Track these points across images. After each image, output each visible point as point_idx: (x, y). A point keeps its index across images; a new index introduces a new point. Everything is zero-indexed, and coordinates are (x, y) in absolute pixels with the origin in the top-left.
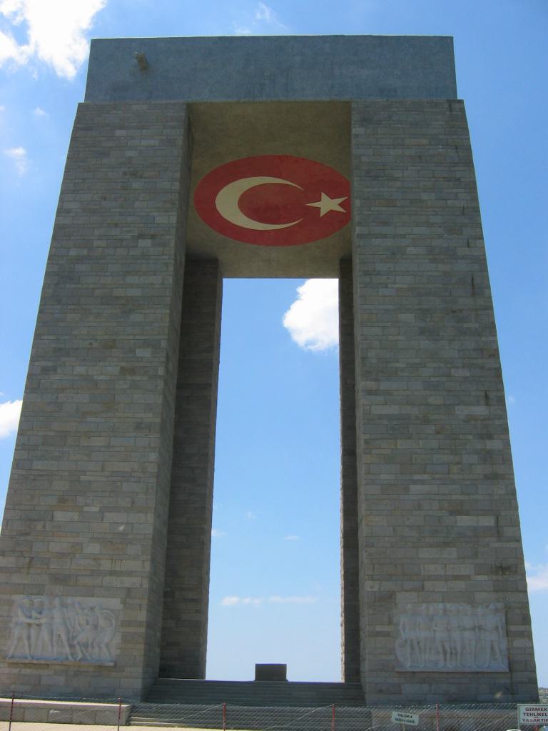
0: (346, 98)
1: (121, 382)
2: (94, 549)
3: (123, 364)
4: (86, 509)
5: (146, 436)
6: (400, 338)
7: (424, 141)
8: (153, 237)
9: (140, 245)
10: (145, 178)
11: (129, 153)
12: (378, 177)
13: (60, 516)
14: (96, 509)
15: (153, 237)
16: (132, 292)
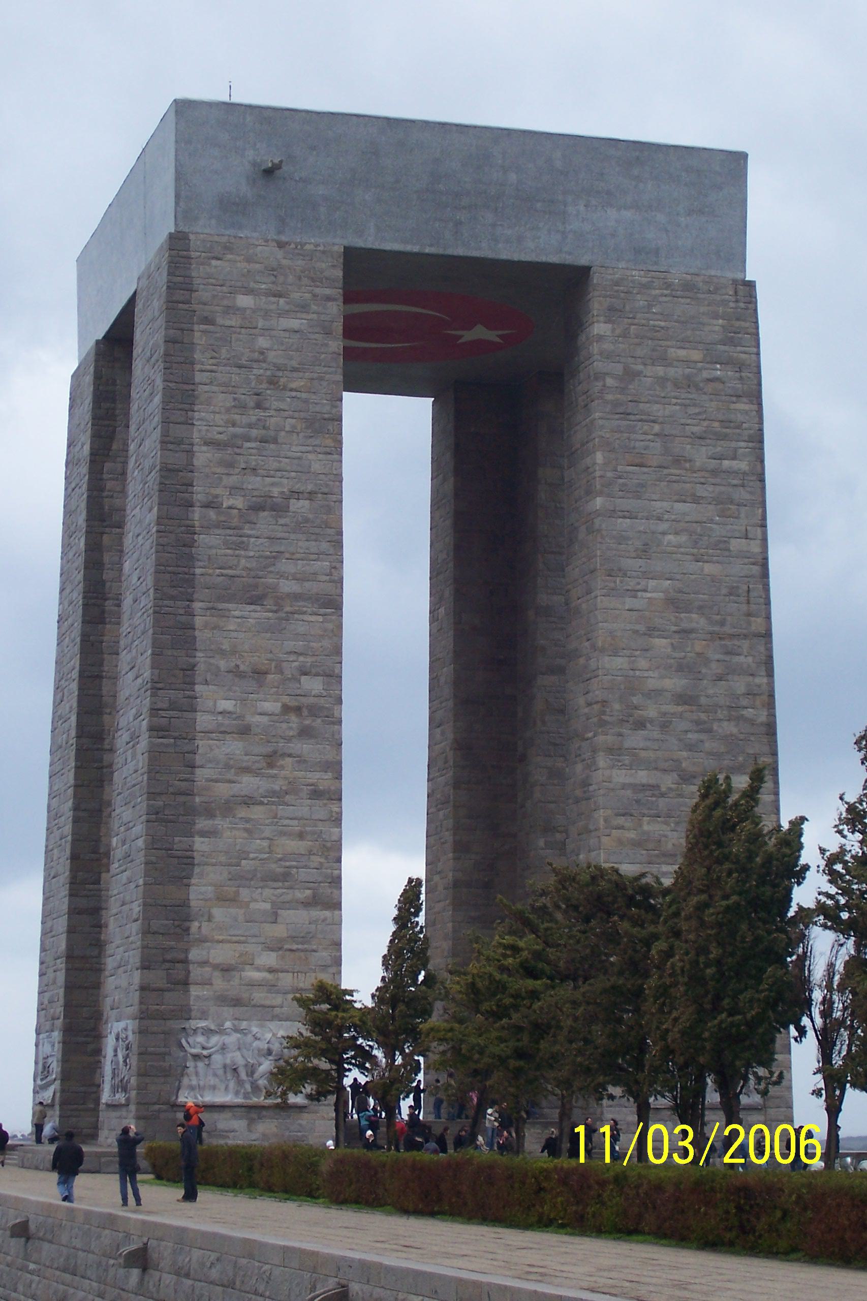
0: (583, 261)
1: (284, 725)
2: (270, 959)
3: (286, 699)
4: (252, 905)
5: (325, 805)
6: (651, 673)
7: (696, 355)
8: (311, 496)
9: (292, 508)
10: (291, 390)
11: (262, 342)
12: (629, 414)
13: (218, 913)
14: (268, 906)
15: (311, 496)
16: (287, 587)
